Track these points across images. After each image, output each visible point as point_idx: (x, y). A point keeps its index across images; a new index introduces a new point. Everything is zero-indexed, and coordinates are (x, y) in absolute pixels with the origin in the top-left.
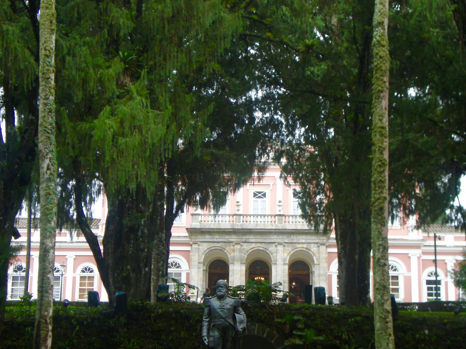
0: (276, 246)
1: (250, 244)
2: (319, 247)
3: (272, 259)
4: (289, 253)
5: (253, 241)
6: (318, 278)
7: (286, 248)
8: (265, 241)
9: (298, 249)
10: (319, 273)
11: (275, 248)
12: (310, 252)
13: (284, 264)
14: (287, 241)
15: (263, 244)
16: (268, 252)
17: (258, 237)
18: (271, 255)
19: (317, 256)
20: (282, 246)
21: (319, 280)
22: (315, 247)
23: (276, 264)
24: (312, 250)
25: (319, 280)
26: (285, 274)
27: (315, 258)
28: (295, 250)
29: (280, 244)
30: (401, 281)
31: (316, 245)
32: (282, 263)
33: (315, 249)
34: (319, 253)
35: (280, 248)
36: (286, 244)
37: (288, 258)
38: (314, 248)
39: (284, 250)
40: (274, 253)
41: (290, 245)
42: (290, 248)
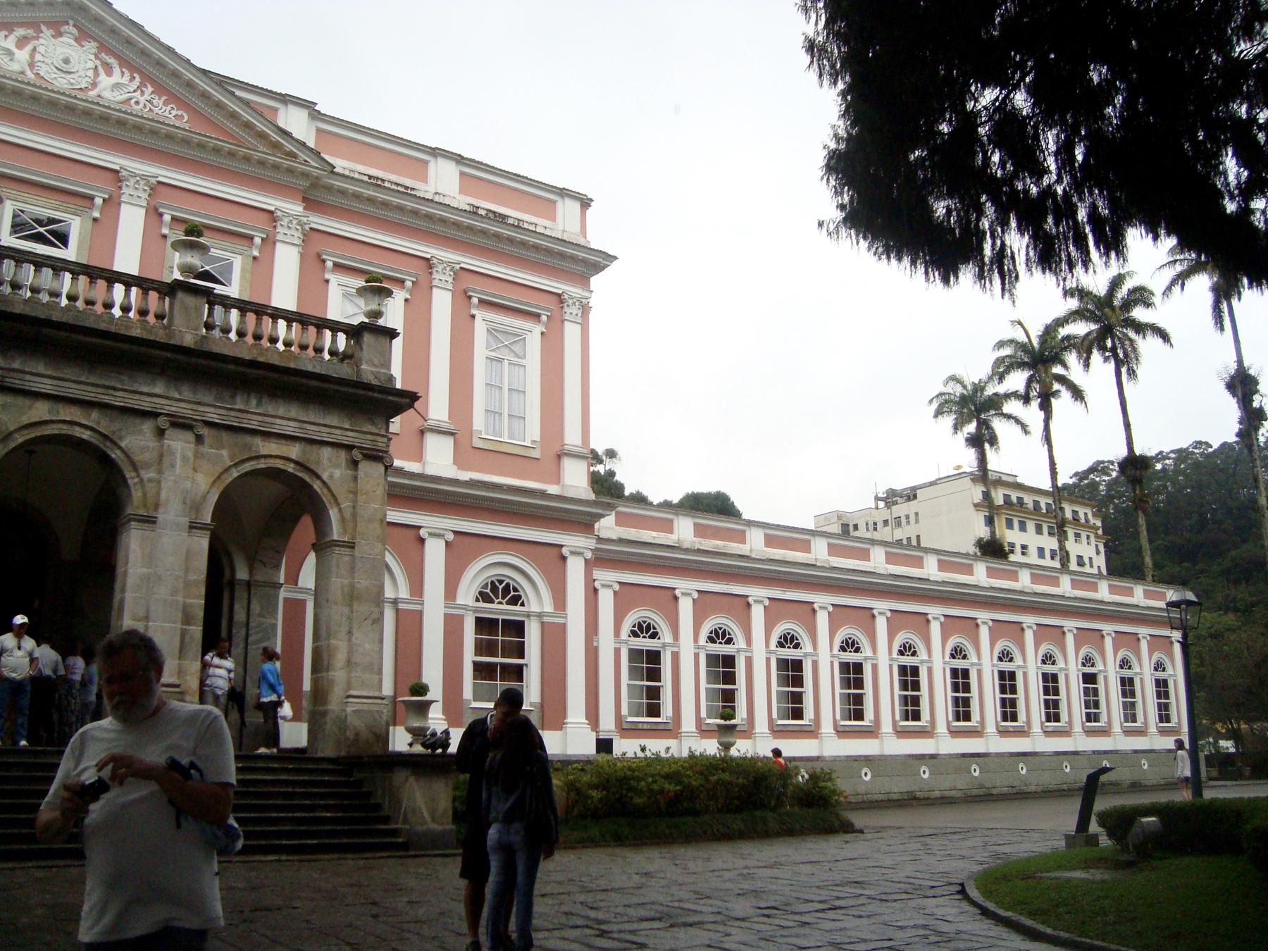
0: (161, 433)
1: (21, 401)
3: (137, 494)
4: (219, 477)
5: (46, 386)
6: (346, 610)
7: (205, 449)
8: (107, 399)
9: (262, 464)
10: (352, 586)
12: (317, 486)
13: (193, 526)
14: (213, 415)
15: (95, 415)
16: (115, 455)
17: (69, 372)
18: (129, 474)
19: (346, 505)
20: (190, 436)
21: (350, 619)
22: (337, 466)
23: (150, 521)
24: (325, 476)
25: (350, 619)
26: (192, 577)
27: (333, 514)
28: (248, 467)
30: (533, 638)
31: (343, 454)
32: (185, 521)
33: (337, 473)
34: (355, 493)
35: (179, 444)
36: (204, 431)
37: (214, 497)
38: (332, 468)
39: (197, 455)
40: (147, 465)
41: (226, 437)
42: (225, 453)
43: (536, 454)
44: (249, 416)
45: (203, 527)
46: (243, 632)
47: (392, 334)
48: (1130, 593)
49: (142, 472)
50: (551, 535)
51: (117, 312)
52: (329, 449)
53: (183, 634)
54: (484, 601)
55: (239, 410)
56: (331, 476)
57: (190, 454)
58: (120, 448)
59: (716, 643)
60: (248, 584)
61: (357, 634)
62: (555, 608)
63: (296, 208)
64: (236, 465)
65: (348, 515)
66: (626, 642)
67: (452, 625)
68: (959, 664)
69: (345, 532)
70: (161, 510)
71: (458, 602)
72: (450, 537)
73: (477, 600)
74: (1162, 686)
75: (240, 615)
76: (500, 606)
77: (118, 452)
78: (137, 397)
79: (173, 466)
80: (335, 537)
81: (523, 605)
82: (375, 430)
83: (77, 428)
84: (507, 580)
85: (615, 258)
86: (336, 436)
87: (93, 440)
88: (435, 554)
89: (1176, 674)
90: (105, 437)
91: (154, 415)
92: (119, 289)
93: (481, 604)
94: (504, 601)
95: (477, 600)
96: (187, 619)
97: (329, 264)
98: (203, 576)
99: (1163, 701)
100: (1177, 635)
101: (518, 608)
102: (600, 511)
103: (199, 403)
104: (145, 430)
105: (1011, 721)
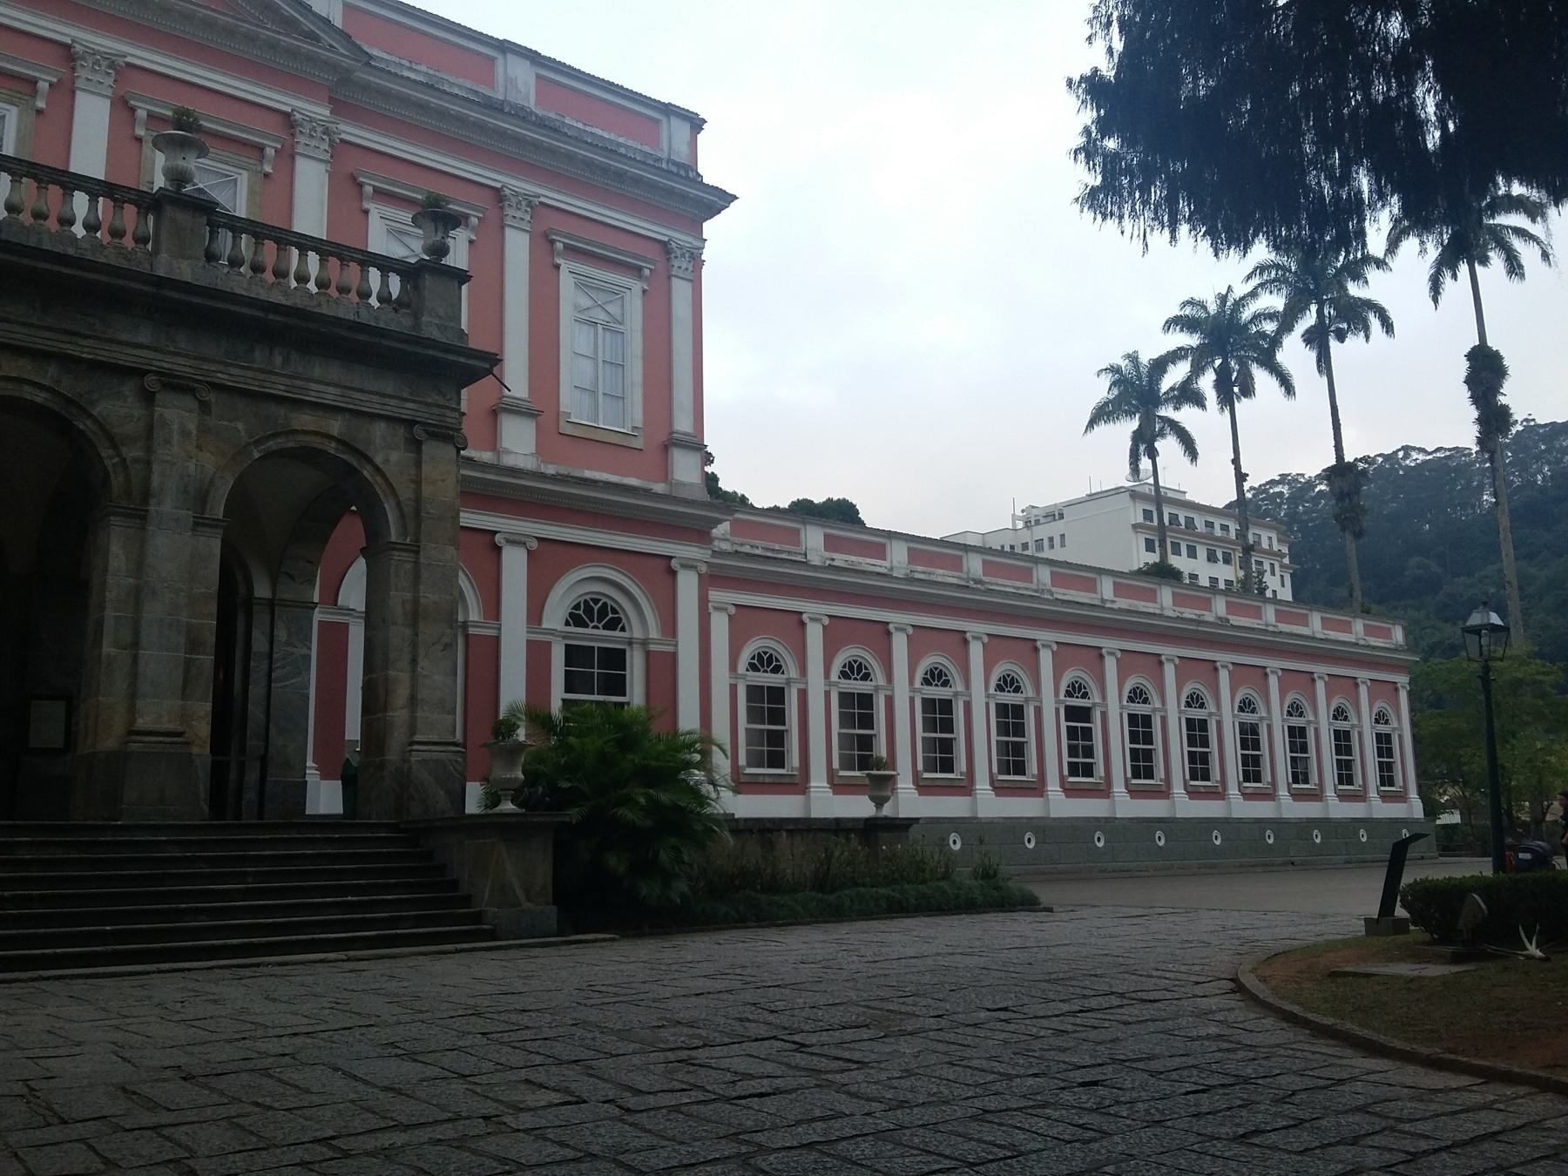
0: (148, 398)
2: (416, 445)
11: (138, 411)
15: (52, 370)
18: (105, 452)
19: (405, 493)
20: (189, 402)
21: (414, 645)
23: (139, 515)
24: (378, 460)
25: (414, 645)
28: (272, 445)
29: (175, 384)
31: (401, 431)
33: (395, 456)
35: (176, 413)
36: (212, 397)
42: (240, 426)
43: (638, 443)
44: (273, 378)
45: (214, 524)
46: (264, 666)
47: (461, 277)
48: (1347, 627)
49: (124, 450)
50: (667, 545)
51: (79, 230)
52: (383, 425)
53: (188, 664)
54: (576, 625)
55: (261, 371)
56: (387, 461)
57: (192, 427)
58: (91, 416)
59: (931, 685)
60: (271, 604)
61: (424, 664)
62: (664, 633)
63: (322, 112)
64: (258, 442)
65: (408, 510)
66: (743, 677)
67: (537, 655)
68: (1140, 709)
69: (404, 534)
70: (153, 501)
71: (545, 625)
72: (534, 545)
73: (567, 624)
74: (1384, 743)
75: (259, 644)
76: (595, 631)
77: (89, 423)
78: (115, 347)
79: (168, 442)
80: (393, 539)
81: (623, 629)
82: (441, 401)
83: (27, 388)
84: (604, 600)
85: (735, 198)
86: (392, 408)
87: (51, 405)
88: (515, 564)
89: (1402, 728)
90: (69, 401)
91: (138, 373)
92: (80, 201)
93: (572, 629)
94: (600, 626)
95: (567, 624)
96: (193, 645)
97: (369, 190)
98: (216, 587)
99: (1386, 760)
100: (1402, 680)
101: (617, 633)
102: (717, 515)
103: (203, 359)
104: (127, 393)
105: (1202, 780)
